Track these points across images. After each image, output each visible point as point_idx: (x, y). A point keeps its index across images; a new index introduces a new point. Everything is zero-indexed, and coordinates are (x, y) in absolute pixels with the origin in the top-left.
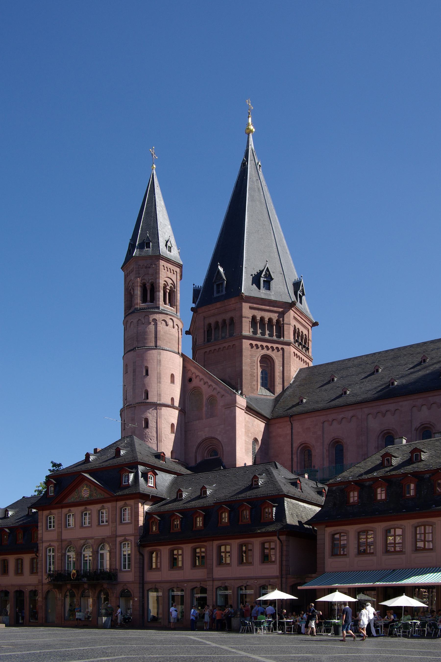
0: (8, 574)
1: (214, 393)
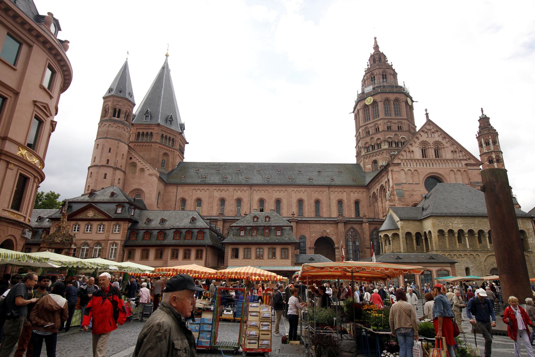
1: (144, 167)
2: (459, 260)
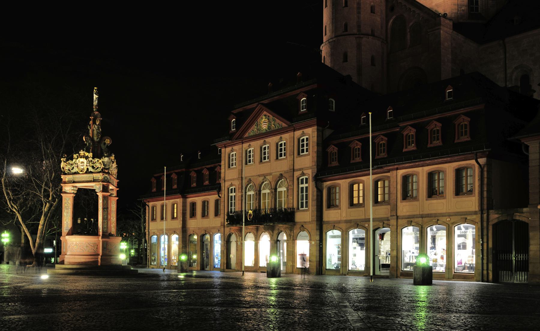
0: (195, 217)
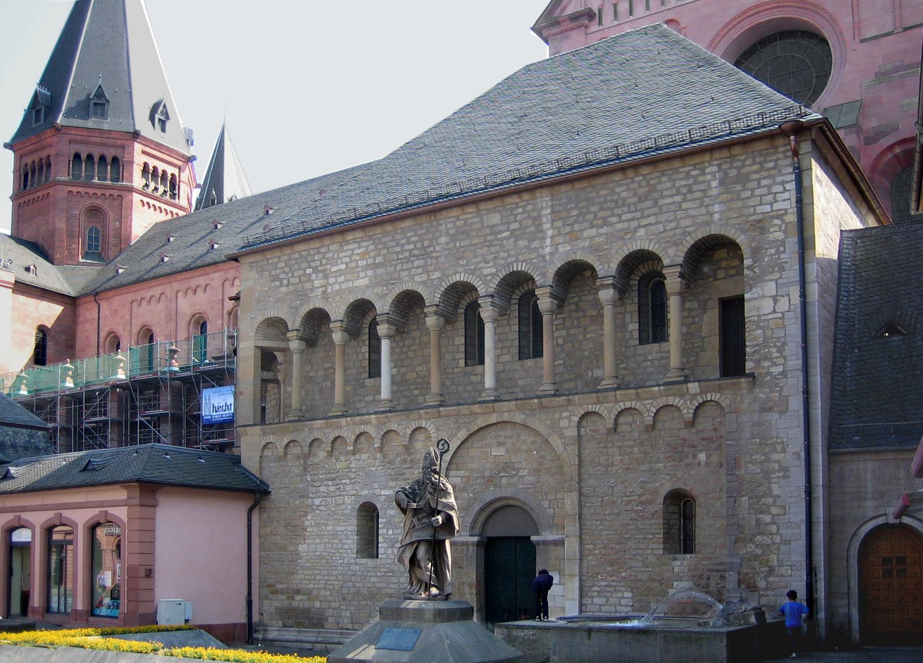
2: (339, 466)
